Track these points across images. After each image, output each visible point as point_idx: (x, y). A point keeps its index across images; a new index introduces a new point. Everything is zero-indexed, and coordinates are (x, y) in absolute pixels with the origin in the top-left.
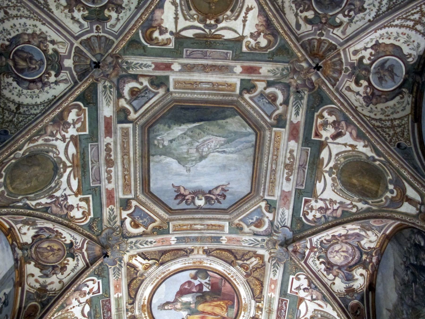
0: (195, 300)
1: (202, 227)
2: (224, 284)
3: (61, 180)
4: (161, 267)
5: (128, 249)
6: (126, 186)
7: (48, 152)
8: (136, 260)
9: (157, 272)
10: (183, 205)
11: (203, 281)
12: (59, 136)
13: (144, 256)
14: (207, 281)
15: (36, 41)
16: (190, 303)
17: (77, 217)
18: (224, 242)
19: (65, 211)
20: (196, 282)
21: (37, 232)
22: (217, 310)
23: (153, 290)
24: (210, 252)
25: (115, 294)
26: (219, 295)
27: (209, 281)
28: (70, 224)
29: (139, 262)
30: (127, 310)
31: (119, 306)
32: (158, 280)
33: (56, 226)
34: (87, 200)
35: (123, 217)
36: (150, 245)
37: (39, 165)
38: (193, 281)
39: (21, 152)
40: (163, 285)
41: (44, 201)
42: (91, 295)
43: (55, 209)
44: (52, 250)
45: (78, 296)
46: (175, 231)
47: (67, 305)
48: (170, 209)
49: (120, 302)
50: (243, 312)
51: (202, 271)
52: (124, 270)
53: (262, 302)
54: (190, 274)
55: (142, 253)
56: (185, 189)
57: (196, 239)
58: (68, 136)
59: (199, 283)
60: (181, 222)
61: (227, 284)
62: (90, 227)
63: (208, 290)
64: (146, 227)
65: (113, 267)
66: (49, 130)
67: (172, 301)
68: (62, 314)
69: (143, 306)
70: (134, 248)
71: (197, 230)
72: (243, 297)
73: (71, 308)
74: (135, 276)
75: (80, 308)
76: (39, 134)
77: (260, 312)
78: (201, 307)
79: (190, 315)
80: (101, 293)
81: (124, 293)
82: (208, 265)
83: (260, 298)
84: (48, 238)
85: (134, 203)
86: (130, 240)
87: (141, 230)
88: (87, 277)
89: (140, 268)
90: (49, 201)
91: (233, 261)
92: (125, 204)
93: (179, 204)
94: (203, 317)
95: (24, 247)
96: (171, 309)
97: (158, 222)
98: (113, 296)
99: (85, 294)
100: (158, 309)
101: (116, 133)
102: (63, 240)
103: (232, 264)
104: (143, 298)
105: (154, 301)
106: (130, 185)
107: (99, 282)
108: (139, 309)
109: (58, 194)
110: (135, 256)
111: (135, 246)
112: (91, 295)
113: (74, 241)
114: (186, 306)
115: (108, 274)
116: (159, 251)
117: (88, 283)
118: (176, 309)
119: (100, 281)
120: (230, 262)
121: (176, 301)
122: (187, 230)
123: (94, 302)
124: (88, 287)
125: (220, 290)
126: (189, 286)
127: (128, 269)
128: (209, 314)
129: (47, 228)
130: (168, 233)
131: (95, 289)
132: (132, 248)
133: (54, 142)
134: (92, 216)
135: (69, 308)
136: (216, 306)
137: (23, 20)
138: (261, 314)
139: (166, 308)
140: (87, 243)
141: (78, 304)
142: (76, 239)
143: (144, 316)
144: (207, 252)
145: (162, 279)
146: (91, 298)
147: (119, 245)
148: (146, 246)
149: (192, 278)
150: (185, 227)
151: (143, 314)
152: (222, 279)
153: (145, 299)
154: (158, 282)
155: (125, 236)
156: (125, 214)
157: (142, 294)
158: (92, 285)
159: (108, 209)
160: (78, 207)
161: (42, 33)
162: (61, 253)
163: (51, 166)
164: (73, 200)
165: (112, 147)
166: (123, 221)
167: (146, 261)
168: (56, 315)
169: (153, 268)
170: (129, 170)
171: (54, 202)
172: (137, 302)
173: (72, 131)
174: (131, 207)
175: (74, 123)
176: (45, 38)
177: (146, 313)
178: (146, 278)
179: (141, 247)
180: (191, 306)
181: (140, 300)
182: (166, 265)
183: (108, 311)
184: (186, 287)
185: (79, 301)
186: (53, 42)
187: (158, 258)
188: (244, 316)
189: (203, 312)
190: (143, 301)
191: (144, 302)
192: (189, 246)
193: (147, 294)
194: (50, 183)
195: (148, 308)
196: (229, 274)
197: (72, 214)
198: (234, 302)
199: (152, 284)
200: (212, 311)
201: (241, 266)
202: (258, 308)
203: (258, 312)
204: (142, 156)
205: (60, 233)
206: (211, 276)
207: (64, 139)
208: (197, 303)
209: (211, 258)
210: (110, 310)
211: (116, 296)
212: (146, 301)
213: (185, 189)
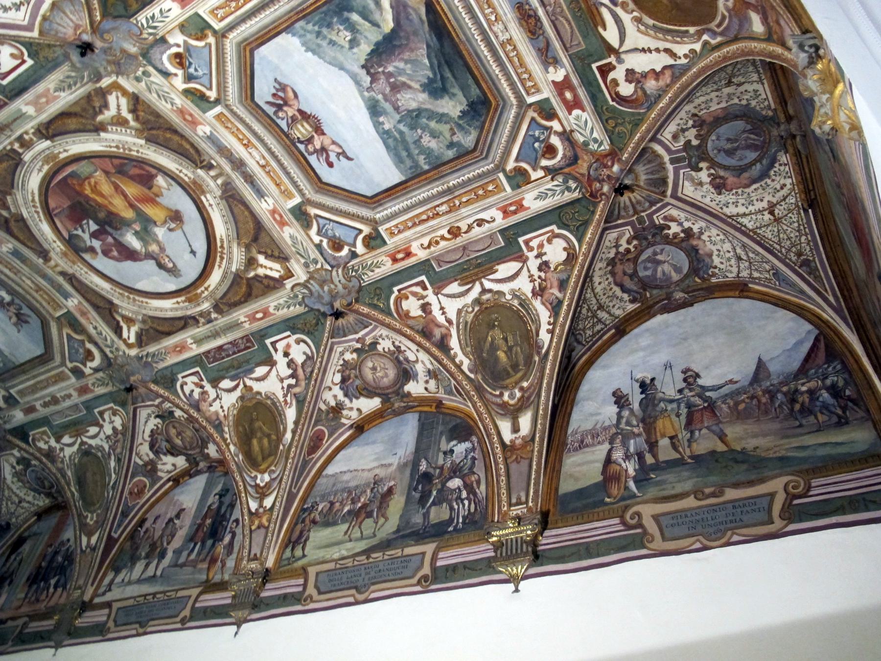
0: (124, 228)
1: (24, 278)
2: (56, 208)
3: (94, 445)
4: (116, 301)
5: (121, 353)
6: (61, 378)
7: (75, 464)
8: (129, 338)
9: (126, 306)
10: (25, 310)
11: (86, 237)
12: (61, 455)
13: (118, 331)
14: (79, 232)
15: (22, 478)
16: (136, 233)
17: (120, 422)
18: (10, 246)
19: (120, 436)
20: (97, 244)
21: (165, 454)
22: (106, 188)
23: (155, 298)
24: (41, 252)
25: (191, 349)
26: (80, 203)
27: (76, 229)
28: (130, 431)
29: (130, 334)
30: (210, 321)
31: (209, 337)
32: (137, 298)
33: (140, 440)
34: (101, 413)
35: (92, 371)
36: (100, 328)
37: (85, 473)
38: (99, 250)
39: (76, 493)
40: (139, 286)
41: (113, 464)
42: (205, 383)
43: (118, 450)
44: (179, 434)
45: (207, 403)
46: (61, 307)
47: (218, 419)
48: (42, 322)
49: (202, 337)
50: (62, 156)
51: (74, 247)
52: (152, 349)
53: (9, 148)
54: (94, 258)
55: (116, 333)
56: (10, 318)
57: (44, 276)
58: (58, 446)
59: (94, 241)
60: (44, 304)
61: (52, 204)
62: (123, 404)
63: (91, 222)
64: (83, 342)
65: (154, 365)
66: (60, 465)
67: (153, 262)
68: (228, 426)
69: (189, 300)
70: (115, 346)
71: (33, 282)
72: (41, 174)
73: (223, 411)
74: (152, 331)
75: (224, 395)
76: (64, 475)
77: (26, 137)
78: (129, 214)
79: (155, 223)
80: (198, 369)
81: (185, 336)
82: (59, 243)
83: (7, 155)
84: (167, 441)
85: (70, 365)
86: (110, 355)
87: (89, 346)
88: (179, 397)
89: (134, 329)
90: (113, 457)
91: (17, 221)
92: (78, 373)
93: (29, 316)
94: (138, 200)
95: (192, 461)
96: (168, 256)
97: (66, 331)
98: (196, 350)
99: (204, 393)
100: (181, 276)
101: (28, 402)
102: (160, 426)
103: (21, 219)
104: (176, 306)
105: (171, 287)
106: (58, 375)
107: (183, 377)
108: (199, 305)
109: (106, 447)
110: (125, 341)
111: (112, 347)
112: (205, 383)
113: (153, 416)
114: (145, 235)
115: (166, 368)
116: (99, 314)
117: (187, 392)
118: (162, 249)
119: (180, 376)
120: (21, 224)
121: (149, 256)
122: (47, 294)
123: (214, 375)
124: (192, 391)
125: (72, 208)
126: (111, 250)
127: (146, 345)
128: (125, 196)
129: (152, 447)
130: (68, 311)
131: (195, 379)
132: (117, 349)
133: (67, 458)
134: (112, 405)
135: (222, 414)
136: (102, 195)
137: (15, 490)
138: (26, 133)
139: (170, 265)
140: (143, 402)
141: (218, 400)
142: (149, 416)
143: (206, 293)
144: (45, 255)
145: (131, 293)
146: (209, 381)
147: (122, 366)
148: (104, 333)
149: (97, 253)
150: (45, 296)
151: (204, 295)
152: (55, 215)
153: (178, 303)
154: (138, 296)
155: (108, 363)
156: (87, 371)
157: (172, 310)
158: (189, 383)
159: (96, 389)
160: (112, 422)
161: (13, 476)
162: (177, 425)
163: (85, 459)
164: (108, 430)
165: (41, 402)
166: (96, 370)
167: (122, 323)
168: (227, 436)
169: (124, 312)
170: (47, 380)
171: (114, 450)
172: (189, 313)
173: (53, 442)
174: (76, 367)
175: (46, 443)
176: (16, 472)
177: (199, 291)
178: (144, 315)
179: (108, 338)
180: (138, 229)
181: (182, 309)
182: (109, 297)
183: (224, 350)
184: (115, 253)
185: (214, 400)
186: (14, 467)
187: (108, 312)
188: (65, 151)
189: (132, 206)
190: (181, 304)
191: (184, 302)
192: (61, 279)
193: (167, 304)
194: (99, 458)
195: (189, 292)
196: (37, 212)
197: (120, 428)
198: (65, 178)
199: (147, 303)
200: (115, 195)
201: (8, 208)
202: (26, 145)
203: (31, 140)
204: (24, 372)
205: (152, 431)
206: (69, 232)
207: (62, 450)
208: (127, 224)
209: (46, 246)
210: (220, 348)
211: (194, 346)
212: (179, 299)
213: (10, 318)
